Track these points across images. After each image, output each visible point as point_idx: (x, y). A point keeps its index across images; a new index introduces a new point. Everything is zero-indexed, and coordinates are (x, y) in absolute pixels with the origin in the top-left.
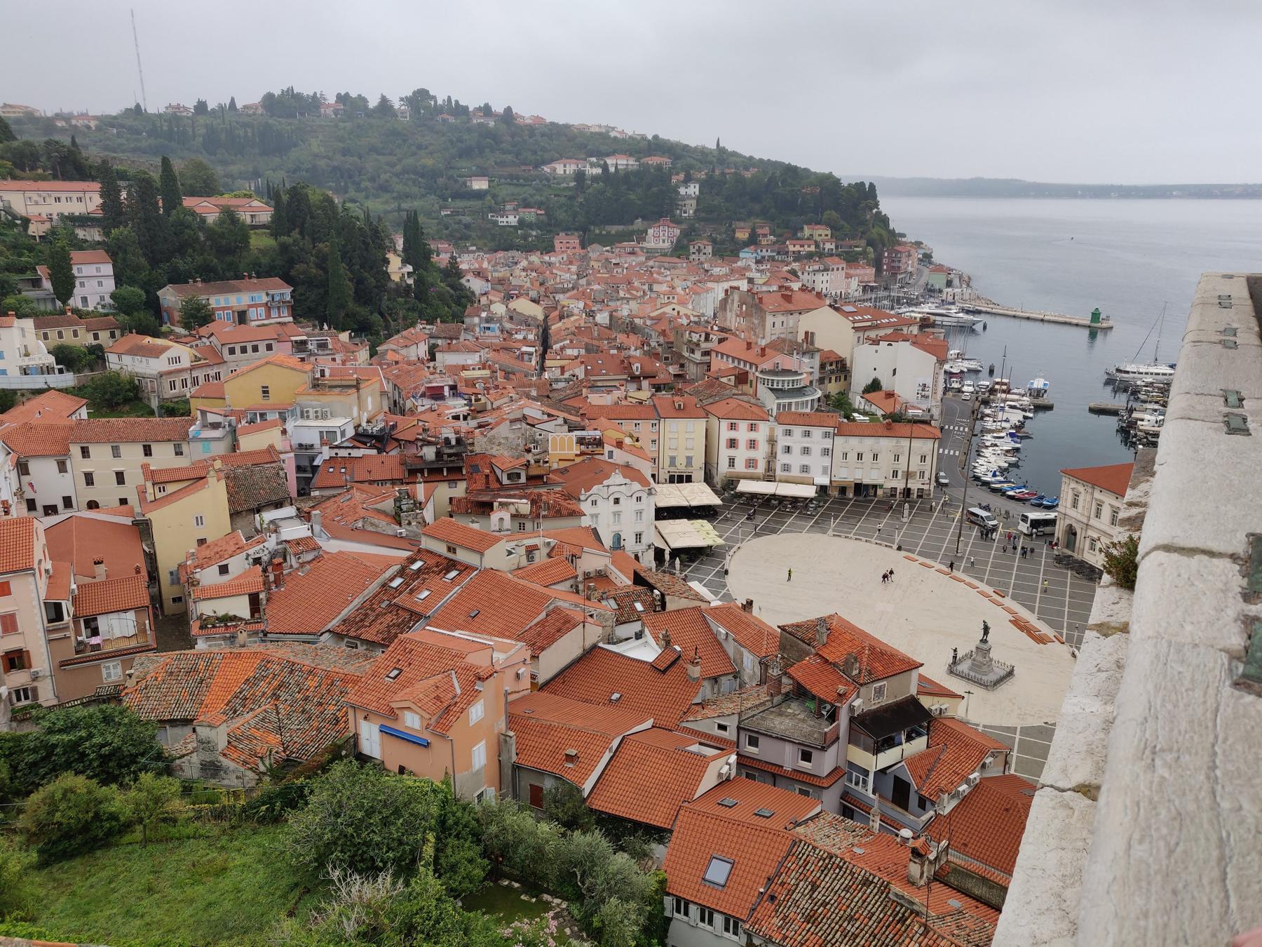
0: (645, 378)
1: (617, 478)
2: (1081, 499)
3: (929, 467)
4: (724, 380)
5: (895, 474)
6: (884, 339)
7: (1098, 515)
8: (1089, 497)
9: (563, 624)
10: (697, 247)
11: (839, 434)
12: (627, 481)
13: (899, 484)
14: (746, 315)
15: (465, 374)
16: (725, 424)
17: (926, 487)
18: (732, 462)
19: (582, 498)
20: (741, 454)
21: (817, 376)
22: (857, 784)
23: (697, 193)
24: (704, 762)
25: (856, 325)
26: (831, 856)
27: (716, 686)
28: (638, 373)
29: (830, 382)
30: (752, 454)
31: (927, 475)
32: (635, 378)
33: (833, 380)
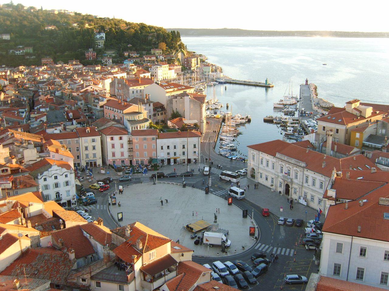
0: (75, 119)
5: (184, 153)
7: (262, 163)
8: (258, 155)
10: (105, 60)
11: (159, 138)
14: (122, 88)
16: (108, 138)
17: (196, 157)
18: (114, 155)
19: (39, 177)
21: (152, 113)
27: (87, 260)
28: (71, 118)
29: (158, 115)
31: (197, 153)
32: (70, 120)
33: (160, 114)
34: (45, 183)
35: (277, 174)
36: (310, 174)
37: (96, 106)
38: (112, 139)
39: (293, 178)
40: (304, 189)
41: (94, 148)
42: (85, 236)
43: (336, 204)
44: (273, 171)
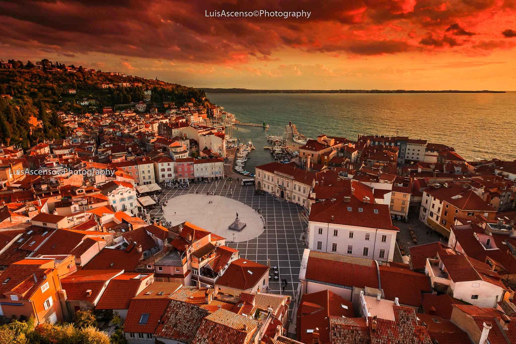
1: (121, 187)
2: (260, 174)
3: (222, 170)
4: (159, 151)
5: (212, 173)
6: (207, 134)
9: (90, 243)
12: (125, 187)
13: (214, 176)
15: (64, 157)
17: (221, 176)
19: (108, 195)
20: (166, 173)
21: (189, 146)
22: (195, 273)
23: (151, 94)
24: (139, 282)
25: (199, 131)
26: (182, 302)
27: (150, 252)
30: (169, 172)
31: (221, 173)
32: (130, 153)
34: (113, 198)
35: (275, 184)
36: (297, 184)
37: (149, 142)
38: (162, 165)
39: (286, 186)
40: (293, 194)
41: (149, 172)
42: (149, 234)
43: (316, 203)
44: (272, 183)
